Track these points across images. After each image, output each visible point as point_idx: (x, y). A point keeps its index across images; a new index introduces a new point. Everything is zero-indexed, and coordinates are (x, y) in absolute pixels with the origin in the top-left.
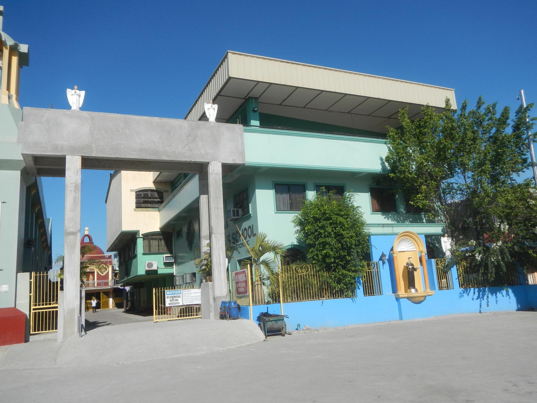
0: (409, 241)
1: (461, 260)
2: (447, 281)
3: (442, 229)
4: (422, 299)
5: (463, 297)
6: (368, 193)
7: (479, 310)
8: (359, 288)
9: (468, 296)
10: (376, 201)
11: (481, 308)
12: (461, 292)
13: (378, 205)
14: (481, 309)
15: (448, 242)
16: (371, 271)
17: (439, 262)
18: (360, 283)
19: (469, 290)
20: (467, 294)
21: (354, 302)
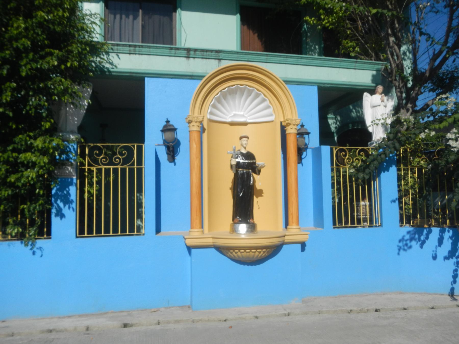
0: (257, 96)
1: (414, 153)
2: (371, 206)
3: (373, 76)
4: (257, 254)
5: (409, 251)
6: (235, 14)
7: (451, 286)
8: (60, 214)
9: (421, 247)
10: (256, 35)
11: (455, 282)
12: (404, 236)
13: (262, 45)
14: (454, 286)
15: (382, 107)
16: (115, 171)
17: (345, 156)
18: (67, 201)
19: (425, 232)
20: (419, 243)
21: (38, 253)
